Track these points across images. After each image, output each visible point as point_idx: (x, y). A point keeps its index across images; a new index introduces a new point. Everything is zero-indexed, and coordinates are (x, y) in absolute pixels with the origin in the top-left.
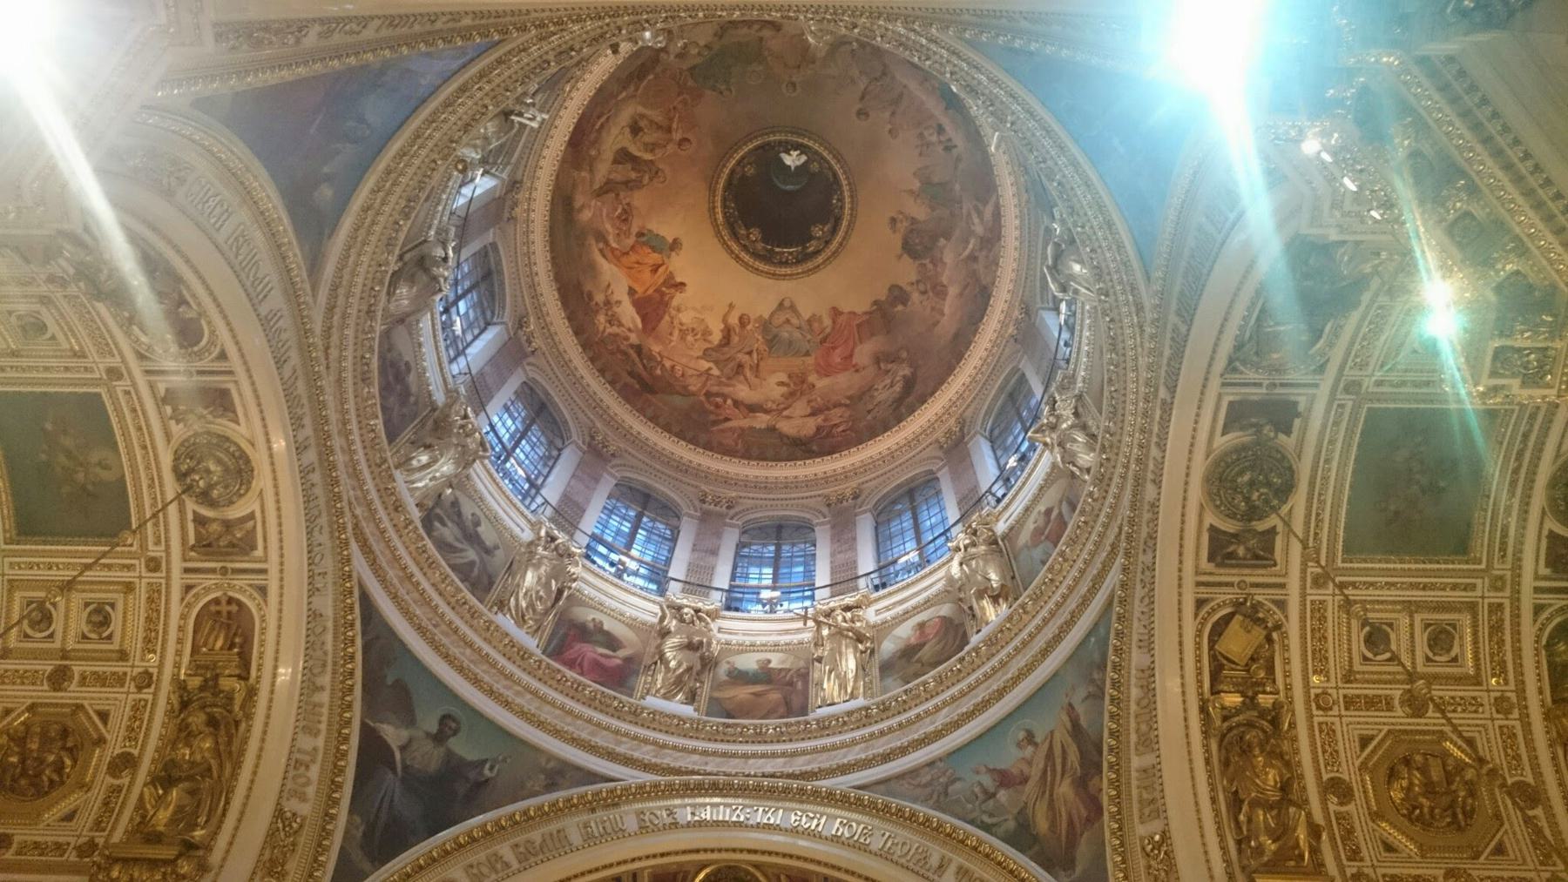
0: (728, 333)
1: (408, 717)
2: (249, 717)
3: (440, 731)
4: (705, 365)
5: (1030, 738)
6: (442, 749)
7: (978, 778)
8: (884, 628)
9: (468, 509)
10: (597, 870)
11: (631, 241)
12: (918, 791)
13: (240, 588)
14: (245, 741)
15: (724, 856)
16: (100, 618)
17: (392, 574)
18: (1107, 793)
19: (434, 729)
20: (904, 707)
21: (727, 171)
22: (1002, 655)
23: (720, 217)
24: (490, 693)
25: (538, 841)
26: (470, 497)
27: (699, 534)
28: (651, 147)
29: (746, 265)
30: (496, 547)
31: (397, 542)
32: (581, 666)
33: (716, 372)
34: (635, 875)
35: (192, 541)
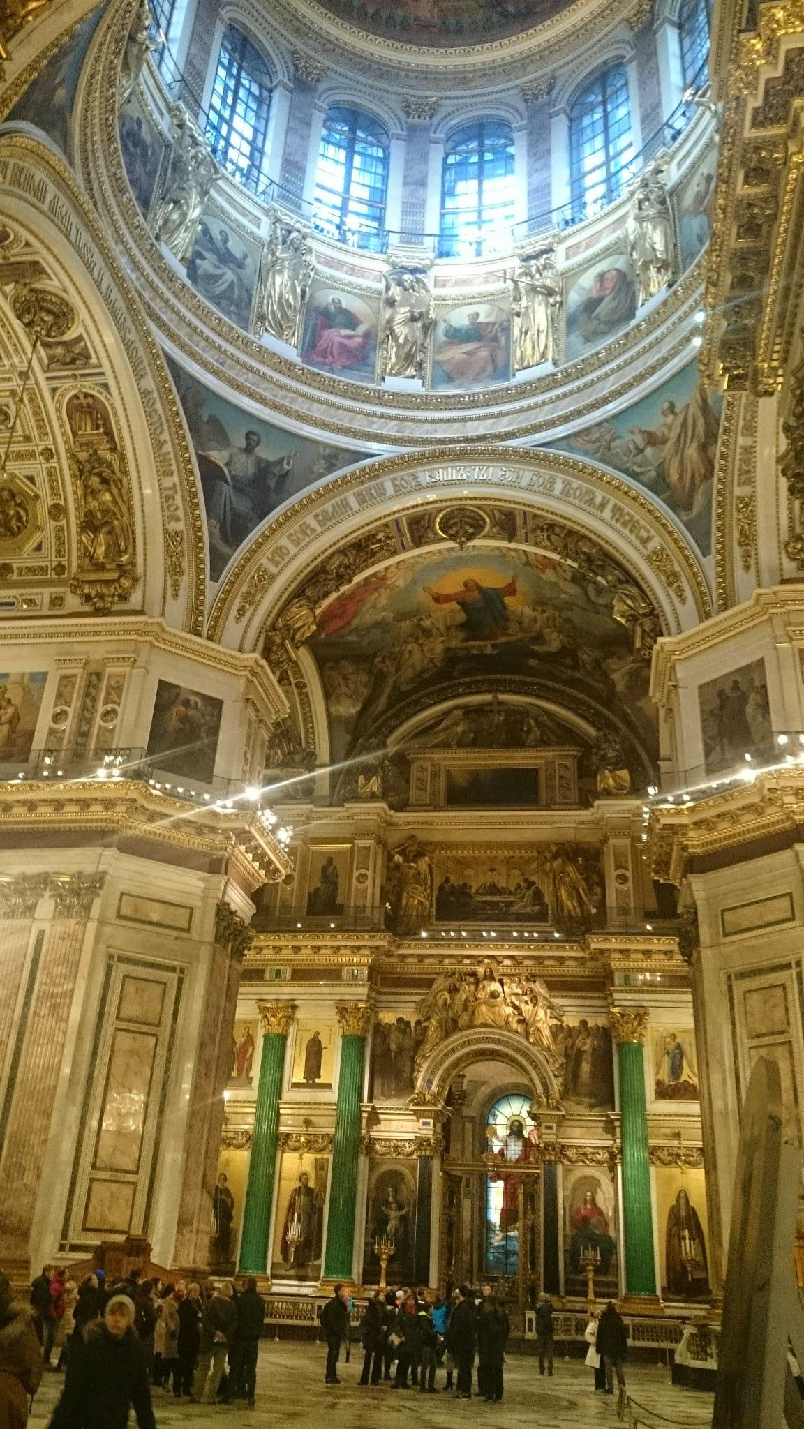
1: (224, 441)
2: (126, 473)
3: (248, 444)
5: (672, 409)
7: (632, 437)
8: (569, 276)
12: (591, 447)
13: (89, 386)
14: (130, 491)
15: (454, 503)
17: (183, 334)
18: (718, 462)
19: (243, 444)
20: (582, 373)
22: (657, 334)
24: (276, 407)
25: (330, 510)
26: (215, 216)
27: (408, 164)
31: (179, 306)
32: (331, 353)
34: (396, 521)
35: (46, 361)
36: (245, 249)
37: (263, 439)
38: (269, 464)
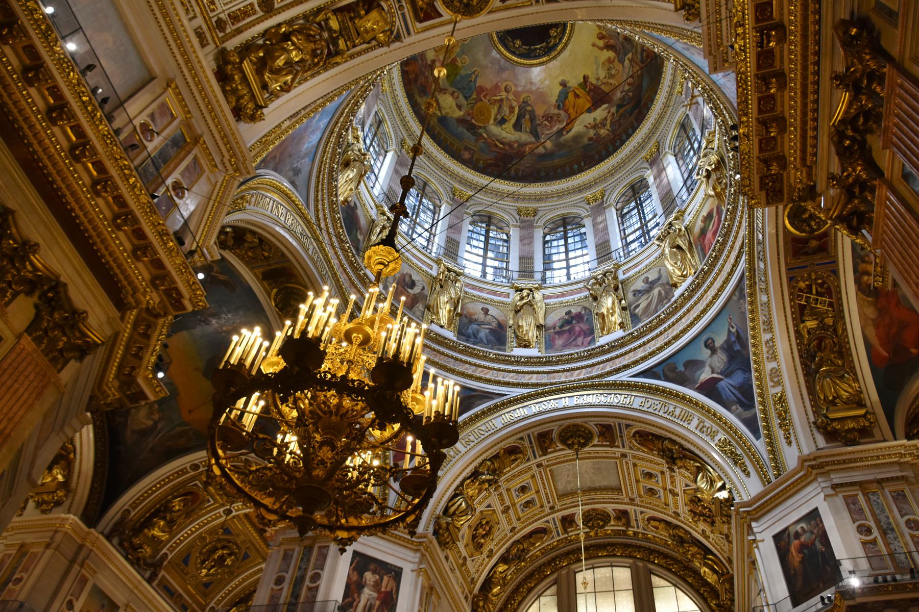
0: (608, 47)
4: (627, 62)
6: (719, 351)
9: (639, 285)
10: (782, 291)
11: (562, 113)
16: (649, 475)
17: (640, 354)
19: (709, 352)
21: (519, 60)
23: (545, 59)
28: (512, 109)
29: (569, 39)
30: (659, 272)
33: (630, 55)
34: (789, 270)
36: (657, 269)
37: (713, 336)
38: (727, 342)
